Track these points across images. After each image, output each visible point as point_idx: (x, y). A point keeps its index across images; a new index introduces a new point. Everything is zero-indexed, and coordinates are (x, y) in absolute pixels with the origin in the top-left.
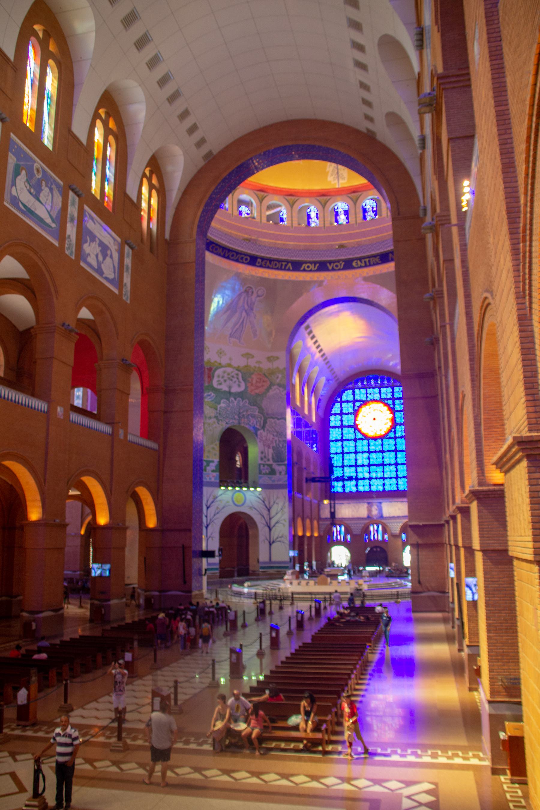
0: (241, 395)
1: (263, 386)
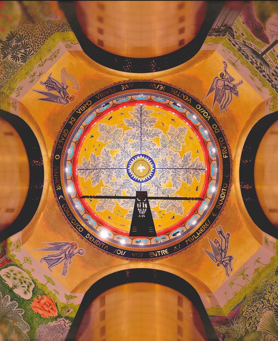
0: (21, 302)
1: (49, 312)
